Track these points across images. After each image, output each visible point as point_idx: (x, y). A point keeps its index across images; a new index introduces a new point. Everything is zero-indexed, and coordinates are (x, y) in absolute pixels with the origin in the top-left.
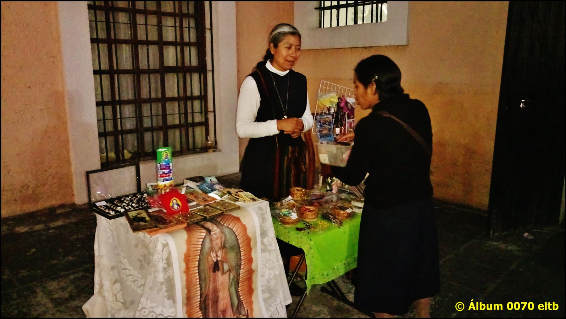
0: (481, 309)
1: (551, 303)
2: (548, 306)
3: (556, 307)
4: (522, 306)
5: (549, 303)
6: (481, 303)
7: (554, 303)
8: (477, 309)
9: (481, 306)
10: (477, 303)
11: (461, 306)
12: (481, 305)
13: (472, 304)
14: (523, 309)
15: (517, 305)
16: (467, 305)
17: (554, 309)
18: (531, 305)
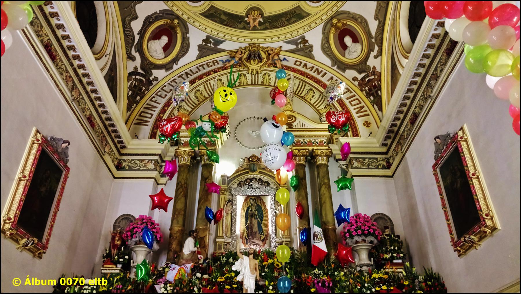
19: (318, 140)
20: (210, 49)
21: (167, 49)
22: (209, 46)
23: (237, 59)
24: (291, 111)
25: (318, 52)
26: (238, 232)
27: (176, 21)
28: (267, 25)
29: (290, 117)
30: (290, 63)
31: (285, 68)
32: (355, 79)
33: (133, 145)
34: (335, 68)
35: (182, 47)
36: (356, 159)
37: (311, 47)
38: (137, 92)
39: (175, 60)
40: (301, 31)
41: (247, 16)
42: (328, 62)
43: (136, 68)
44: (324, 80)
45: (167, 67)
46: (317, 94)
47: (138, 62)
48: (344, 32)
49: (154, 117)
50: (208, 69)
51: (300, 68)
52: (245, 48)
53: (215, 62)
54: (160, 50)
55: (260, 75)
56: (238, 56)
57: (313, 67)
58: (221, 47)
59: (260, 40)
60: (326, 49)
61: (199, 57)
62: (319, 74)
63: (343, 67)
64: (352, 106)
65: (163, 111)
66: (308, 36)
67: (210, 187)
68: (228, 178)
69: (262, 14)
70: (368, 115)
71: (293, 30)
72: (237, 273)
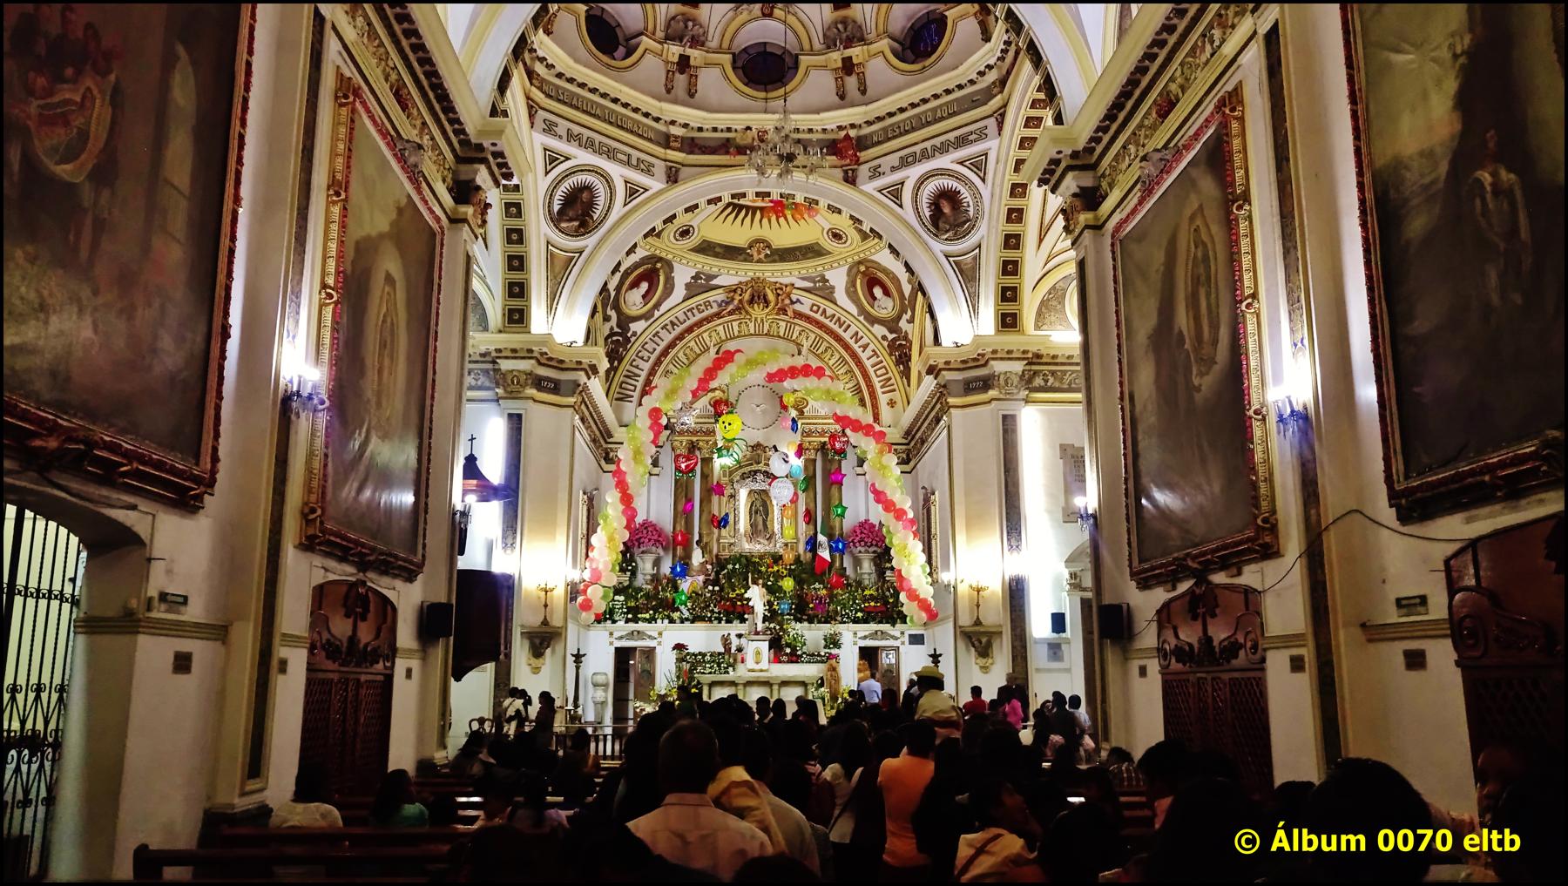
0: (1305, 848)
1: (1501, 832)
2: (1490, 841)
3: (1512, 843)
4: (1419, 839)
5: (1495, 832)
6: (1305, 831)
7: (1507, 831)
8: (1296, 848)
9: (1307, 841)
10: (1296, 831)
11: (1251, 841)
12: (1305, 837)
13: (1281, 833)
14: (1422, 848)
15: (1405, 836)
16: (1268, 839)
17: (1507, 848)
18: (1444, 837)
22: (701, 284)
26: (742, 531)
30: (804, 309)
31: (799, 315)
38: (614, 356)
39: (657, 306)
41: (750, 247)
42: (854, 310)
44: (847, 336)
45: (646, 316)
48: (872, 282)
50: (699, 316)
51: (817, 316)
53: (708, 304)
54: (639, 299)
56: (737, 298)
58: (714, 282)
60: (851, 293)
63: (873, 320)
67: (713, 490)
69: (769, 246)
71: (810, 266)
72: (749, 600)
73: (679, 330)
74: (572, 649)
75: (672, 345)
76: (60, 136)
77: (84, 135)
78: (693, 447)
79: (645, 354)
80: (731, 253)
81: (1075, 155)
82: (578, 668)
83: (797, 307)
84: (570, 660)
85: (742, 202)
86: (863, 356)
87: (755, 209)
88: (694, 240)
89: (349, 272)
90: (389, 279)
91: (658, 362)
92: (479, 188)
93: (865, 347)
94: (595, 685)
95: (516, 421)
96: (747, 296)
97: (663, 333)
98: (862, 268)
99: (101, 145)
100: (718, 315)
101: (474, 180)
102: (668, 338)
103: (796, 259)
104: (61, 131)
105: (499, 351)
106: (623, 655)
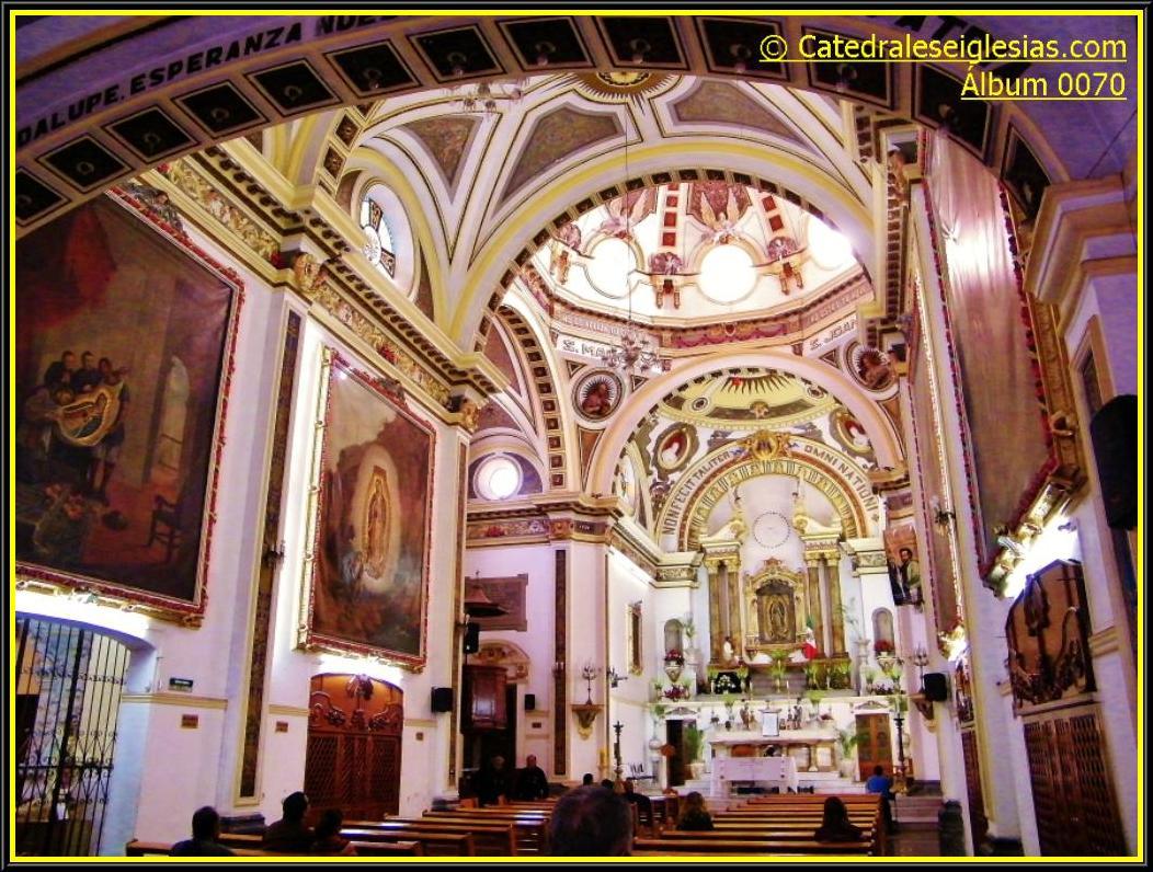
19: (828, 542)
20: (720, 441)
21: (678, 453)
22: (718, 440)
23: (747, 450)
24: (803, 514)
25: (827, 437)
27: (684, 429)
28: (773, 414)
29: (800, 522)
30: (800, 450)
31: (796, 455)
32: (865, 466)
33: (666, 559)
34: (846, 453)
35: (692, 446)
36: (864, 557)
37: (820, 431)
38: (658, 502)
39: (688, 459)
40: (808, 418)
41: (752, 407)
42: (839, 447)
43: (654, 480)
44: (835, 468)
45: (680, 468)
46: (829, 485)
47: (656, 473)
49: (678, 523)
50: (720, 464)
51: (812, 455)
52: (754, 435)
55: (773, 466)
57: (823, 453)
58: (730, 437)
59: (769, 427)
60: (835, 435)
61: (710, 452)
62: (830, 461)
63: (854, 454)
64: (863, 497)
65: (685, 518)
66: (816, 422)
68: (752, 578)
69: (766, 406)
70: (876, 507)
71: (801, 417)
73: (705, 476)
74: (613, 723)
75: (701, 488)
76: (80, 423)
77: (97, 421)
78: (722, 566)
79: (682, 497)
80: (738, 414)
81: (884, 322)
82: (618, 735)
83: (795, 449)
84: (613, 730)
85: (738, 376)
86: (850, 482)
87: (750, 381)
88: (708, 408)
89: (334, 469)
90: (378, 471)
91: (692, 502)
92: (466, 401)
93: (850, 475)
94: (652, 748)
95: (561, 556)
96: (755, 445)
97: (694, 480)
98: (839, 415)
99: (111, 422)
100: (734, 462)
101: (462, 396)
102: (698, 482)
103: (789, 413)
104: (81, 420)
105: (547, 506)
106: (674, 728)
